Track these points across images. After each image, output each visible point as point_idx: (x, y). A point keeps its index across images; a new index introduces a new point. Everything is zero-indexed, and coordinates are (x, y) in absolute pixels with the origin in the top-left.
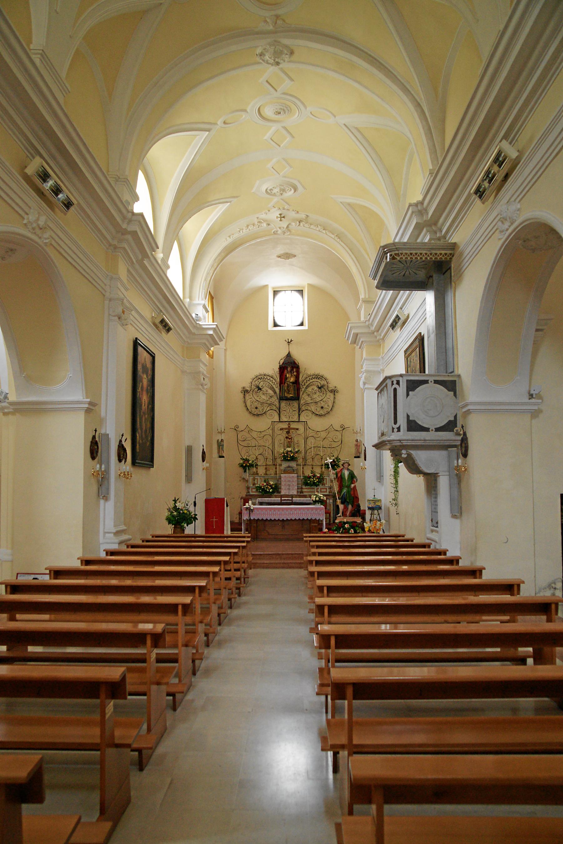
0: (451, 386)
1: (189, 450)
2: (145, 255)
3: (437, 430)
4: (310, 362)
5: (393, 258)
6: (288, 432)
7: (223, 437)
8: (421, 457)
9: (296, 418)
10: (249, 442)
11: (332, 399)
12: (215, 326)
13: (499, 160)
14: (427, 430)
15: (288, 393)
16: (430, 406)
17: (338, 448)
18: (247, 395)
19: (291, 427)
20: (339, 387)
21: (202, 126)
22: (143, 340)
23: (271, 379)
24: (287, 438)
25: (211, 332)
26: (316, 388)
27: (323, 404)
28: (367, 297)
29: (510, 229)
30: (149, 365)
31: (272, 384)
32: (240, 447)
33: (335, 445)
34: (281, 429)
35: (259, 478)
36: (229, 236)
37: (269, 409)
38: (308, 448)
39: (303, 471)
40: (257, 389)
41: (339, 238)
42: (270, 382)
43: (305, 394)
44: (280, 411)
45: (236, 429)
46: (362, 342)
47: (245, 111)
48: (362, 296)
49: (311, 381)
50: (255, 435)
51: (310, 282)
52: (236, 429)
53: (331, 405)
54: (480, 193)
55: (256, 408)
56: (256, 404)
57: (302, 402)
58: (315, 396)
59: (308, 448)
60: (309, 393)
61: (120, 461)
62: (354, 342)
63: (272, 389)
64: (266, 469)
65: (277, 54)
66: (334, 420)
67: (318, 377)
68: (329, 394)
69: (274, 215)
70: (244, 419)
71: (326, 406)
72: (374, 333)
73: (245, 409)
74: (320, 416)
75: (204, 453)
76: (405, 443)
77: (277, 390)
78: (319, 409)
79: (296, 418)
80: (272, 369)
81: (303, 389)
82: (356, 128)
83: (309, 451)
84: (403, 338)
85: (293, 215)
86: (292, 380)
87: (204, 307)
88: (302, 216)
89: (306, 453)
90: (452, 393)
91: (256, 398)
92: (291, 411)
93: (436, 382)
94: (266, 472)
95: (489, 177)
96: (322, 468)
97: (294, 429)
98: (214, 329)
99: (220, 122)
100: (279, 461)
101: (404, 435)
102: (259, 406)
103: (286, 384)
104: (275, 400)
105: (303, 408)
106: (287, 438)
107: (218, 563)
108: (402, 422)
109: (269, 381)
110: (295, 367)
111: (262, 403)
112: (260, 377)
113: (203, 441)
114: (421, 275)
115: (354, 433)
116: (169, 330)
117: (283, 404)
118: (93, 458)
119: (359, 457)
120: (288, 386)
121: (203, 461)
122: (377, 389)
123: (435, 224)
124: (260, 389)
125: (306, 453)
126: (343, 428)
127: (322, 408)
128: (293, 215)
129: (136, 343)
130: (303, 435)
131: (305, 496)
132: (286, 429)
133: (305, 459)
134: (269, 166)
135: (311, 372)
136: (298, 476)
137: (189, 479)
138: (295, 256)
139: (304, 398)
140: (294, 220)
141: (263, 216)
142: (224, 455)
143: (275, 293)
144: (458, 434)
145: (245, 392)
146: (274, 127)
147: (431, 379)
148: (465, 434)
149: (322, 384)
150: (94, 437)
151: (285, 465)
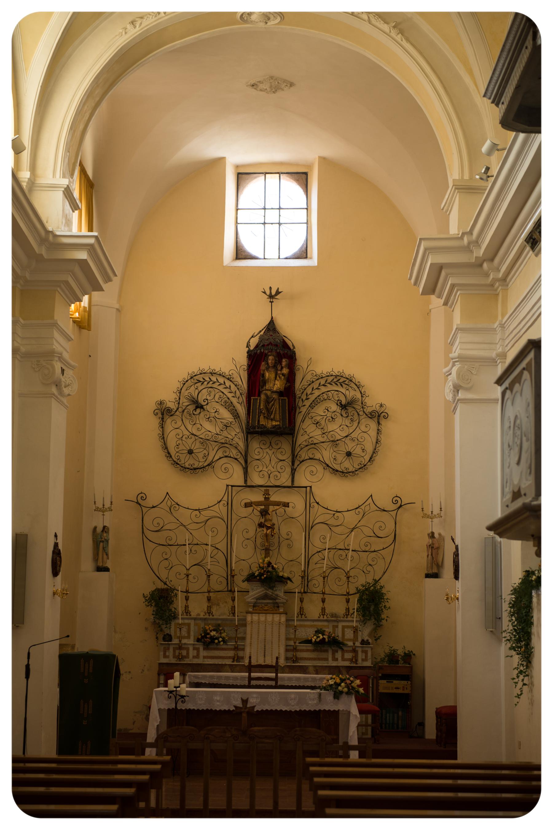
6: (264, 513)
7: (108, 520)
9: (285, 479)
10: (171, 534)
11: (373, 433)
12: (92, 241)
15: (267, 418)
17: (386, 553)
18: (169, 421)
19: (273, 498)
23: (228, 383)
24: (261, 525)
25: (83, 255)
26: (334, 407)
27: (350, 446)
28: (466, 177)
31: (230, 395)
32: (150, 546)
33: (377, 544)
34: (247, 505)
35: (192, 622)
36: (133, 23)
37: (220, 454)
38: (312, 550)
39: (301, 609)
40: (193, 407)
41: (401, 32)
42: (226, 391)
43: (308, 422)
44: (246, 462)
46: (453, 286)
48: (455, 172)
49: (323, 389)
50: (185, 516)
52: (139, 502)
53: (369, 449)
55: (190, 452)
56: (190, 443)
57: (301, 439)
58: (332, 427)
59: (312, 550)
60: (318, 418)
62: (431, 289)
64: (209, 599)
66: (377, 485)
67: (341, 380)
68: (365, 421)
71: (358, 451)
72: (481, 265)
73: (162, 454)
74: (344, 474)
75: (56, 553)
77: (242, 410)
78: (340, 458)
79: (285, 479)
80: (229, 357)
81: (304, 410)
83: (316, 558)
86: (279, 385)
87: (68, 193)
89: (308, 563)
91: (189, 427)
92: (274, 460)
94: (209, 608)
96: (348, 601)
97: (278, 504)
98: (90, 248)
102: (196, 447)
103: (263, 396)
104: (236, 434)
105: (303, 455)
106: (261, 525)
109: (221, 388)
110: (285, 356)
111: (204, 442)
112: (200, 378)
115: (425, 516)
119: (436, 576)
120: (268, 400)
121: (55, 573)
122: (499, 382)
124: (202, 407)
125: (308, 563)
126: (399, 504)
127: (349, 454)
130: (302, 519)
131: (303, 670)
132: (258, 504)
133: (305, 577)
135: (323, 367)
136: (287, 620)
138: (292, 85)
139: (308, 431)
142: (109, 564)
143: (242, 177)
145: (164, 412)
149: (349, 398)
151: (256, 591)
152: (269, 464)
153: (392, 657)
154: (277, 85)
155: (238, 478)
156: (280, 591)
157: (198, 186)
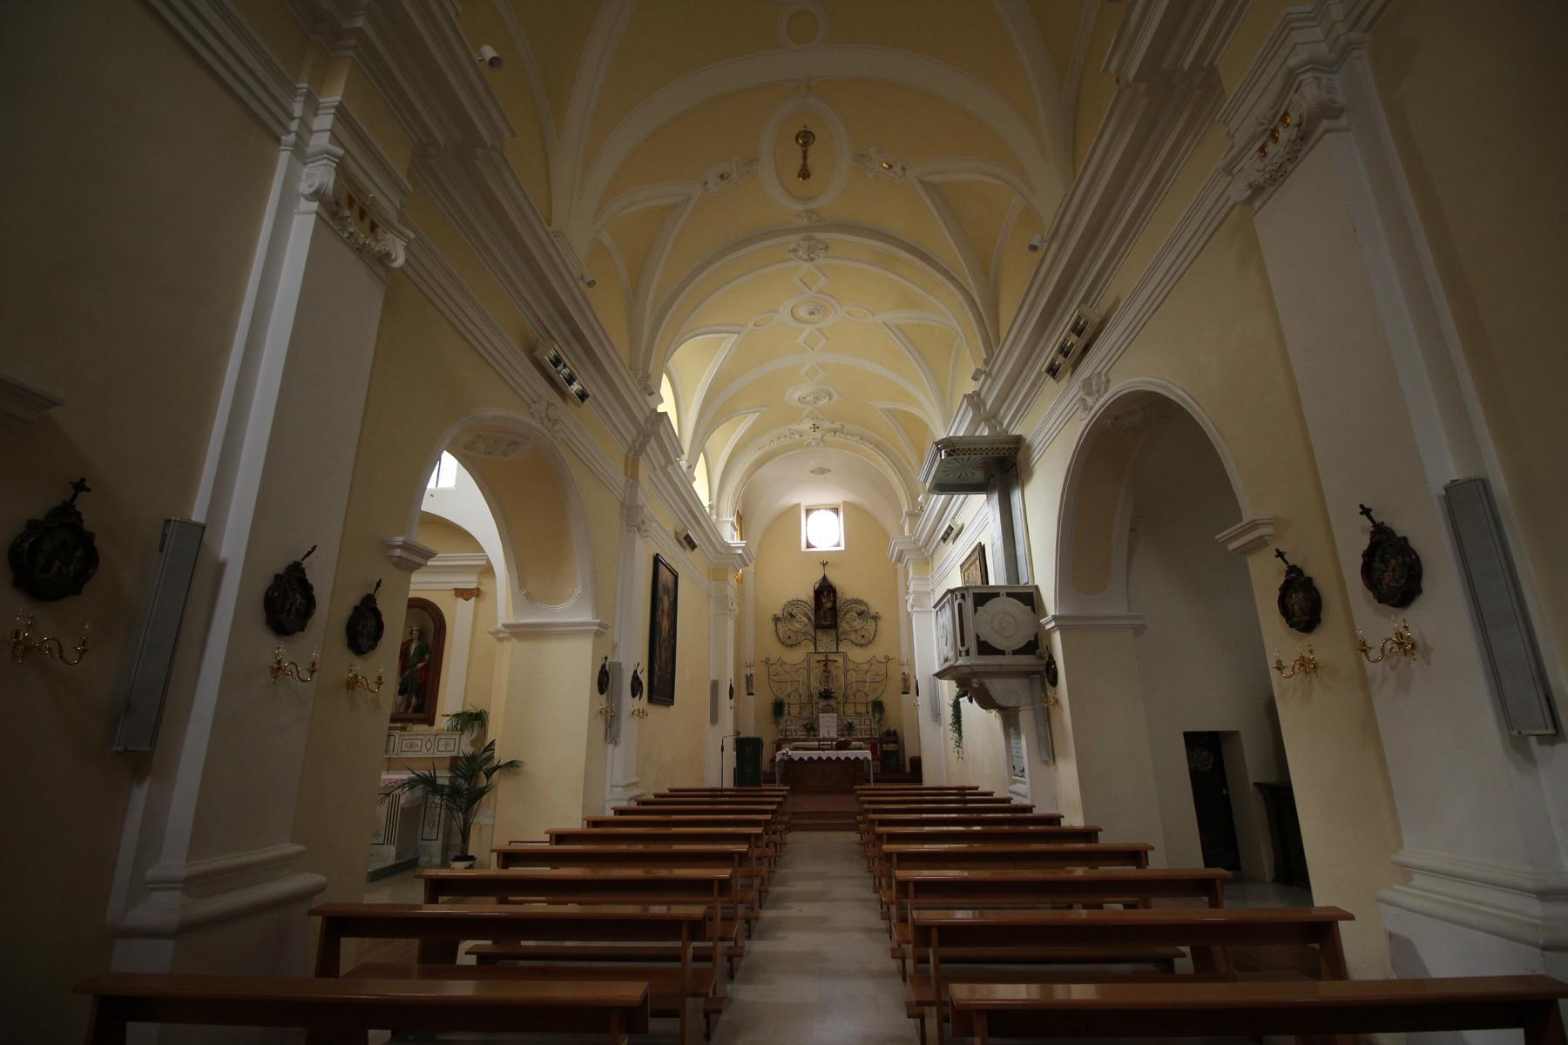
0: (1030, 598)
1: (715, 686)
2: (669, 461)
3: (1015, 652)
4: (848, 586)
5: (948, 455)
8: (997, 687)
13: (1077, 330)
14: (1002, 653)
16: (1003, 624)
20: (881, 612)
21: (732, 328)
22: (665, 557)
29: (1098, 404)
30: (670, 585)
45: (767, 662)
47: (776, 311)
48: (905, 509)
50: (788, 668)
51: (850, 497)
52: (767, 662)
54: (1053, 371)
61: (634, 695)
63: (806, 615)
65: (810, 250)
66: (877, 651)
69: (806, 426)
70: (776, 651)
74: (861, 646)
76: (977, 669)
80: (806, 592)
82: (898, 327)
84: (959, 551)
85: (827, 425)
88: (837, 425)
90: (1029, 608)
93: (1009, 595)
95: (1064, 351)
99: (750, 325)
100: (816, 698)
101: (975, 660)
107: (756, 823)
108: (972, 644)
113: (730, 674)
114: (979, 476)
116: (693, 546)
117: (819, 633)
118: (602, 691)
123: (995, 417)
128: (827, 425)
129: (657, 560)
134: (803, 371)
135: (849, 596)
137: (714, 719)
139: (844, 626)
140: (829, 430)
141: (796, 427)
143: (808, 511)
144: (1041, 657)
145: (777, 619)
146: (808, 329)
147: (1002, 592)
148: (1051, 657)
150: (604, 666)
151: (822, 703)
152: (826, 642)
153: (888, 733)
154: (822, 471)
155: (812, 649)
156: (833, 702)
157: (790, 519)
